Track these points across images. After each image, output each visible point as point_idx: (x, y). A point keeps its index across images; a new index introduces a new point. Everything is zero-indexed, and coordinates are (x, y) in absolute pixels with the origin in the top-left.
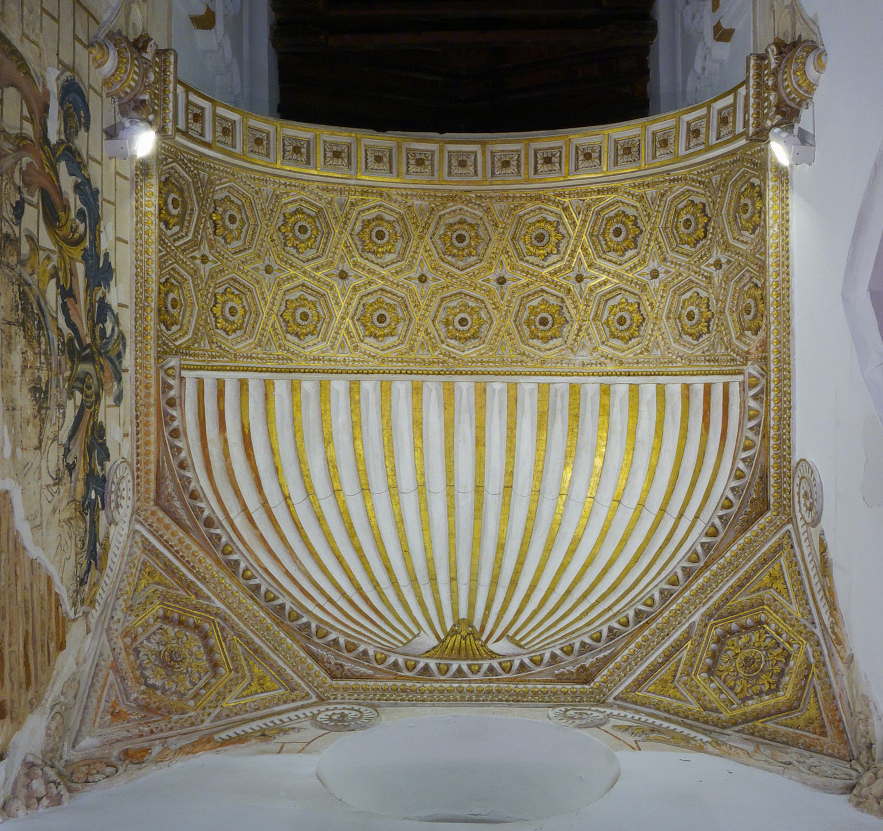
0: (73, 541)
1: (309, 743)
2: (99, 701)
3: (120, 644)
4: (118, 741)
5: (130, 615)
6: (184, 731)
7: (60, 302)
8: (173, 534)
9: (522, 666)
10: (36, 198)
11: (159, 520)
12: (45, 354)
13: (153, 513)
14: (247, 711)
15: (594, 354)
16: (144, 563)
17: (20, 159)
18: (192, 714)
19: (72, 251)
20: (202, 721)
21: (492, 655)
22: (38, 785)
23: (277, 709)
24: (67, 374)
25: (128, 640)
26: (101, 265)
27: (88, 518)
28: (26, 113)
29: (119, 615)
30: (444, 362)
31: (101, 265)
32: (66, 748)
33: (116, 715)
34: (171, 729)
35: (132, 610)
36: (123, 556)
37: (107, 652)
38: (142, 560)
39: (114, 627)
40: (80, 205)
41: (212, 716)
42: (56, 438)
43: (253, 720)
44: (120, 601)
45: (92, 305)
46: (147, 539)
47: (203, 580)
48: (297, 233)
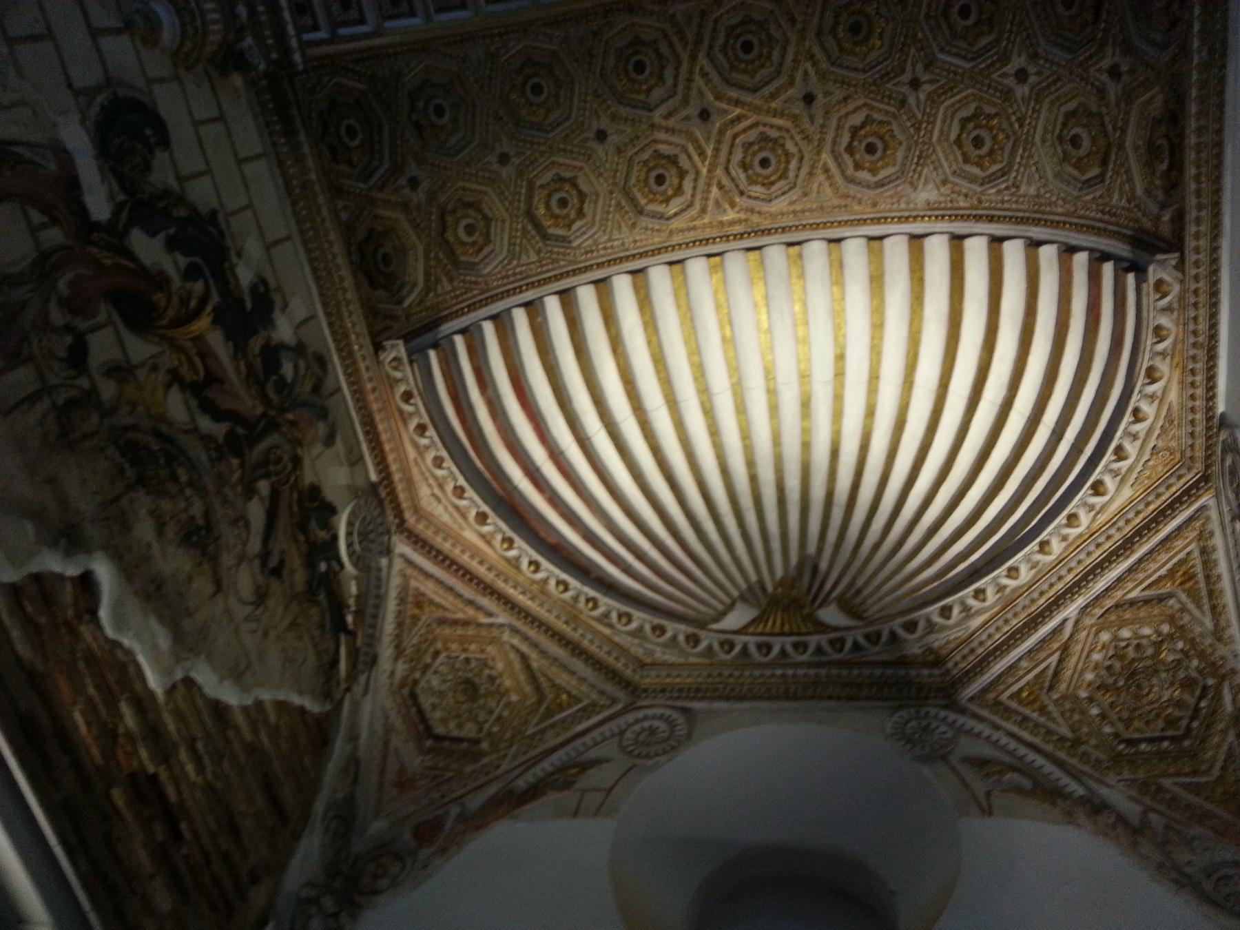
1: (610, 790)
7: (194, 403)
9: (856, 647)
10: (104, 311)
12: (191, 484)
15: (943, 190)
19: (193, 328)
20: (498, 767)
21: (821, 627)
24: (236, 476)
26: (249, 305)
27: (322, 597)
30: (746, 220)
31: (249, 305)
40: (183, 261)
42: (242, 558)
43: (554, 750)
45: (249, 366)
48: (531, 97)
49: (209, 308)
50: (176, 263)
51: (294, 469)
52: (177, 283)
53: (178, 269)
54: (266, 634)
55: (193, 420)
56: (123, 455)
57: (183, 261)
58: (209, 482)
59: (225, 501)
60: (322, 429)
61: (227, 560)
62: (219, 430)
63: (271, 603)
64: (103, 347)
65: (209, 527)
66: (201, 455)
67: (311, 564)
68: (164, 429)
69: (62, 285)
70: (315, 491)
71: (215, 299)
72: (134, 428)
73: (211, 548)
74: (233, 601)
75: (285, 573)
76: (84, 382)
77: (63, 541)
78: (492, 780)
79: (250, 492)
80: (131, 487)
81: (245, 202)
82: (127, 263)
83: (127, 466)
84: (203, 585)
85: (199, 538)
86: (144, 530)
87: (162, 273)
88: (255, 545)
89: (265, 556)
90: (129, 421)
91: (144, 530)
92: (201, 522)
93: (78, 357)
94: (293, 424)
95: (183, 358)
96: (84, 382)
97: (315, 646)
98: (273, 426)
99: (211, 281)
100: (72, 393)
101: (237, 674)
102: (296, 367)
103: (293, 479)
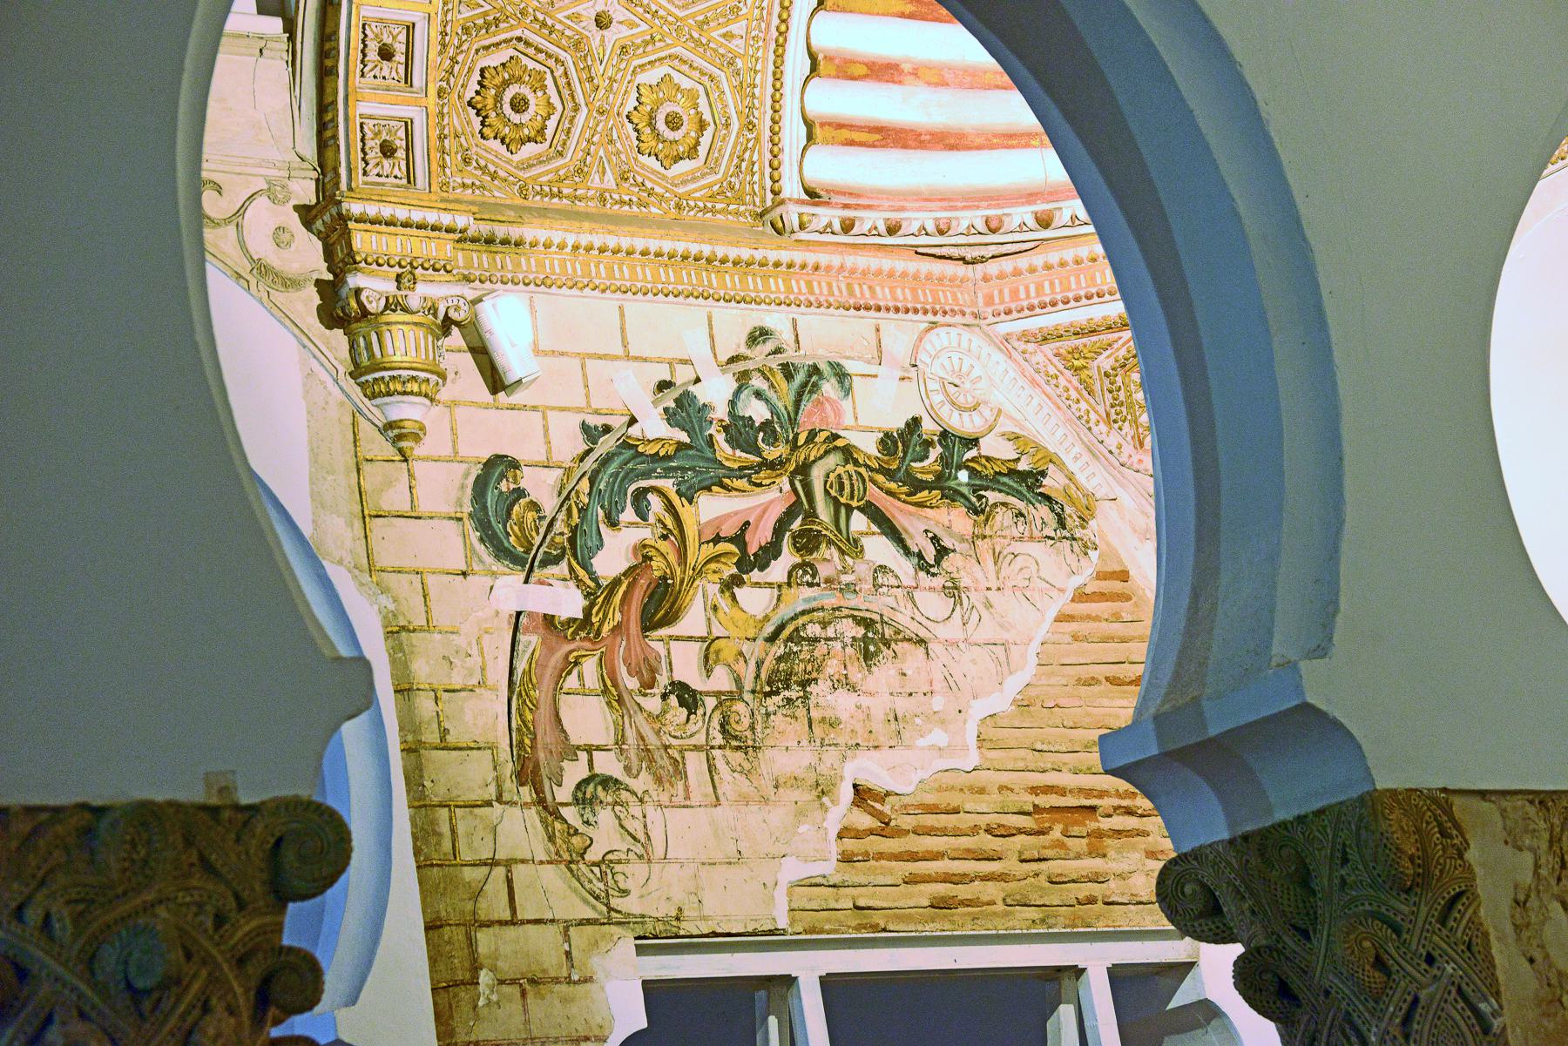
0: (1018, 547)
7: (756, 575)
8: (1032, 270)
10: (656, 642)
11: (1001, 276)
12: (824, 625)
13: (986, 279)
16: (1056, 355)
17: (630, 692)
26: (684, 437)
27: (992, 496)
28: (571, 682)
29: (1112, 440)
31: (684, 437)
36: (1034, 382)
38: (1050, 354)
39: (1124, 459)
44: (1095, 429)
46: (1026, 337)
51: (856, 463)
52: (645, 534)
54: (988, 605)
55: (770, 585)
56: (777, 693)
57: (629, 515)
58: (831, 600)
59: (851, 588)
60: (829, 388)
61: (903, 619)
62: (788, 557)
63: (964, 582)
64: (686, 665)
65: (868, 624)
66: (801, 597)
67: (952, 496)
68: (769, 629)
69: (632, 683)
70: (888, 442)
71: (668, 485)
72: (759, 665)
73: (888, 632)
74: (942, 631)
75: (947, 542)
76: (711, 702)
77: (825, 799)
79: (853, 547)
80: (806, 697)
81: (576, 363)
82: (624, 587)
83: (787, 694)
84: (913, 658)
85: (874, 640)
86: (842, 704)
88: (904, 568)
89: (923, 566)
90: (752, 664)
91: (842, 704)
92: (861, 631)
93: (687, 697)
94: (812, 435)
95: (713, 566)
96: (711, 702)
98: (804, 469)
100: (715, 724)
101: (1006, 666)
102: (758, 394)
103: (862, 470)
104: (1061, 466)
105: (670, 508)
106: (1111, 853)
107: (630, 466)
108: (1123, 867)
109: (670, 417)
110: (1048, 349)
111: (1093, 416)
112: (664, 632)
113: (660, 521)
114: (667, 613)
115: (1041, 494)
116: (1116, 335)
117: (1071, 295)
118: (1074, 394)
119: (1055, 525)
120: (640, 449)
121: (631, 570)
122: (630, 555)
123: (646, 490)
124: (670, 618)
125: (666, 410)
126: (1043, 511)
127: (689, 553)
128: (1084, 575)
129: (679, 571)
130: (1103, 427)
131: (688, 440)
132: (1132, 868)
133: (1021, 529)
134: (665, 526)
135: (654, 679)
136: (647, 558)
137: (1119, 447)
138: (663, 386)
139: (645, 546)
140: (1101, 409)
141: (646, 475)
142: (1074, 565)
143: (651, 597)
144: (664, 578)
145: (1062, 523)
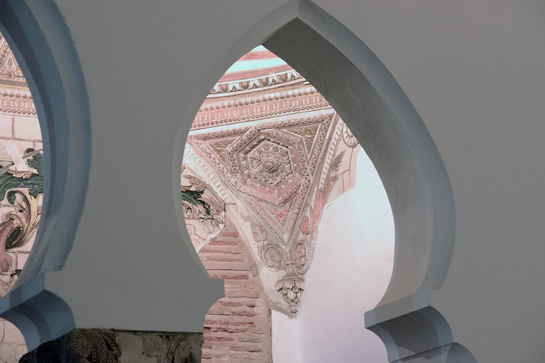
1: (349, 170)
2: (270, 219)
3: (248, 190)
4: (294, 226)
5: (236, 176)
6: (308, 192)
14: (319, 155)
16: (211, 145)
18: (303, 181)
20: (309, 181)
22: (291, 295)
23: (327, 137)
25: (249, 181)
29: (233, 180)
31: (35, 171)
32: (283, 247)
33: (280, 215)
34: (303, 199)
35: (234, 173)
36: (201, 156)
37: (249, 198)
41: (310, 174)
43: (324, 156)
44: (226, 175)
47: (237, 120)
49: (28, 197)
50: (5, 206)
52: (12, 209)
53: (8, 206)
57: (5, 201)
71: (26, 191)
78: (312, 187)
87: (7, 215)
97: (193, 218)
99: (18, 189)
104: (211, 189)
105: (26, 199)
106: (214, 347)
107: (8, 182)
108: (219, 352)
109: (30, 163)
110: (207, 142)
111: (225, 170)
112: (16, 249)
113: (20, 204)
114: (18, 242)
115: (200, 201)
116: (233, 138)
117: (214, 121)
118: (217, 161)
119: (205, 213)
120: (14, 175)
121: (4, 223)
122: (4, 218)
123: (15, 192)
124: (18, 245)
125: (28, 160)
126: (200, 207)
127: (32, 218)
128: (216, 233)
129: (26, 225)
130: (229, 175)
131: (37, 173)
132: (224, 353)
133: (189, 214)
134: (22, 207)
135: (8, 268)
136: (12, 219)
137: (236, 183)
138: (29, 150)
139: (11, 214)
140: (229, 168)
141: (16, 186)
142: (211, 231)
143: (12, 235)
144: (19, 228)
145: (208, 212)
